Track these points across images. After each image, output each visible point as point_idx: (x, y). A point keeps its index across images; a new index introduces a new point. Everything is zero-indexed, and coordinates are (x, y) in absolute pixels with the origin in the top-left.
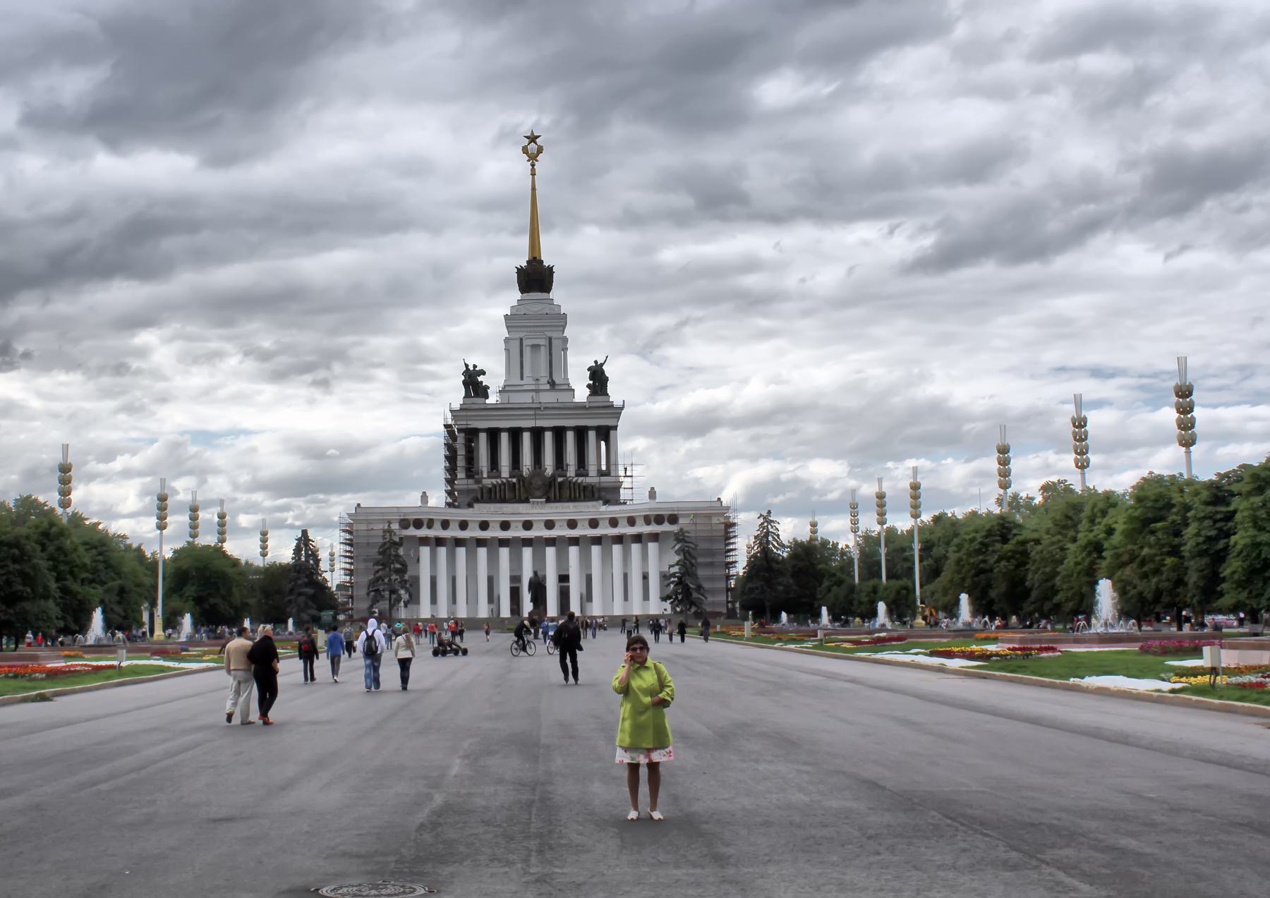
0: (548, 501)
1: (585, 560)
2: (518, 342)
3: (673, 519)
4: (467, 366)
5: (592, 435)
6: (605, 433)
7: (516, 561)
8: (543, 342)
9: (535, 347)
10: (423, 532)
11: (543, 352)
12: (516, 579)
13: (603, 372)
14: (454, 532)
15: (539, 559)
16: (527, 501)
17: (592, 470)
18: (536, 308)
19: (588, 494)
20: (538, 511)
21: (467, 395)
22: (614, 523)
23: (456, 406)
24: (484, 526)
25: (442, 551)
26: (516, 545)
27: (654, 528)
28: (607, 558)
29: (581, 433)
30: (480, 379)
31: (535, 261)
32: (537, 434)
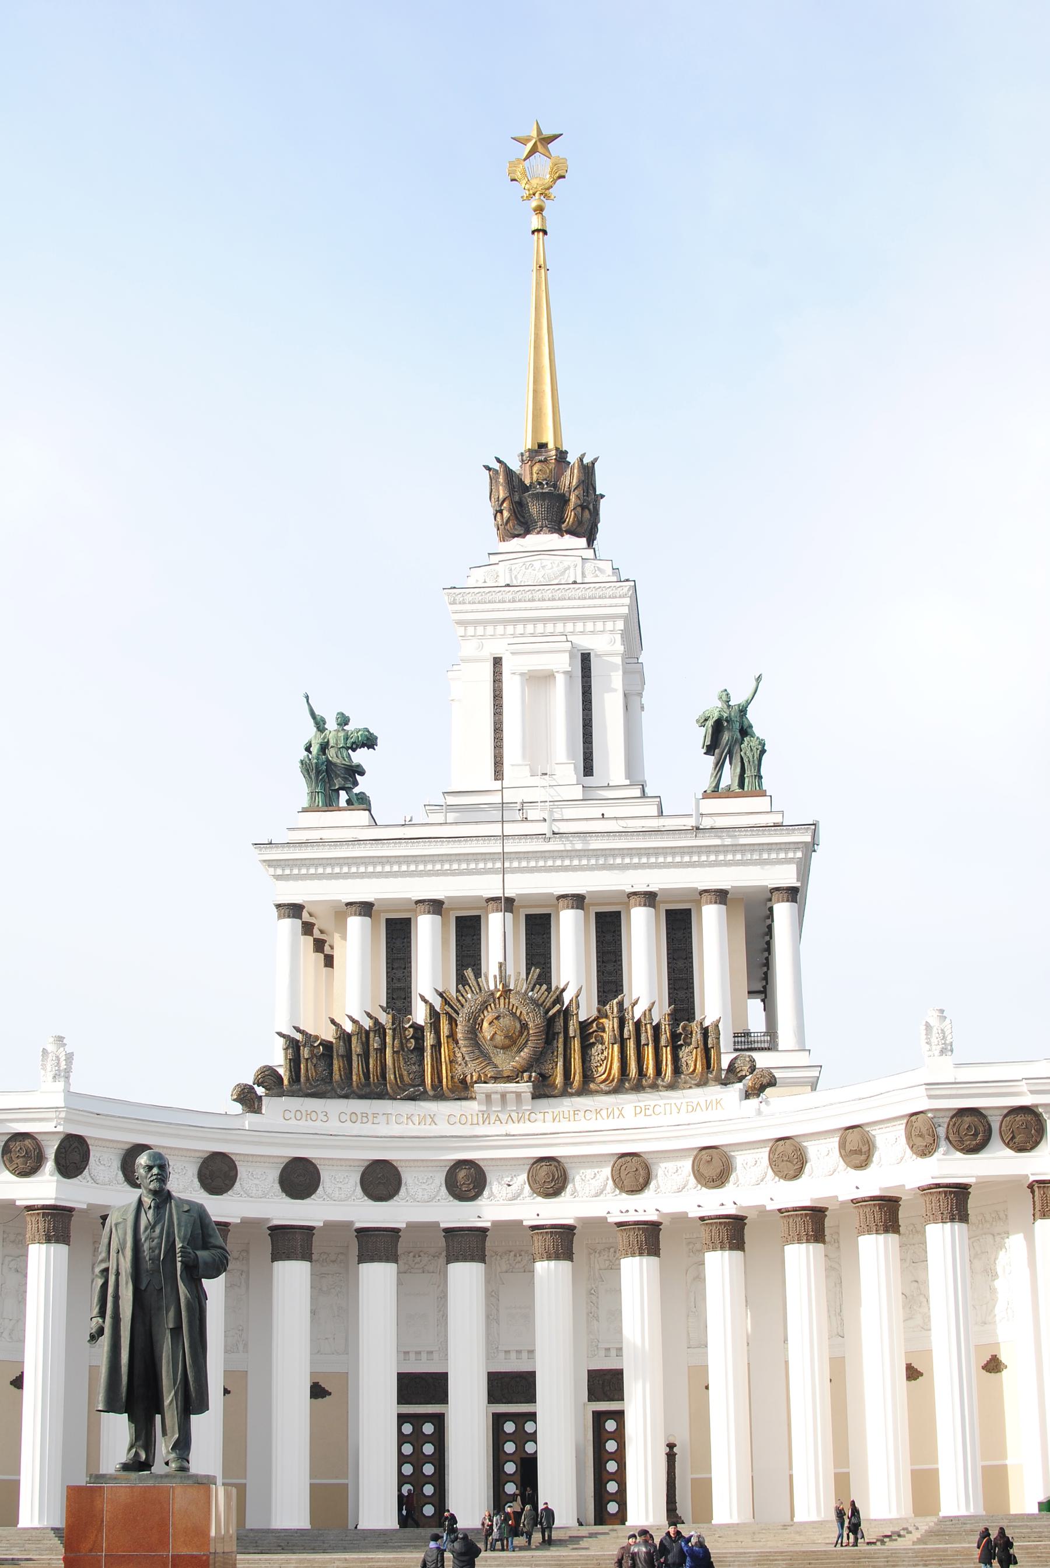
0: (543, 1090)
1: (683, 1304)
2: (489, 667)
3: (1026, 1128)
4: (320, 724)
7: (421, 1311)
8: (562, 663)
10: (45, 1188)
12: (423, 1388)
13: (745, 731)
16: (462, 1090)
19: (690, 1056)
20: (502, 1125)
22: (789, 1158)
24: (300, 1178)
27: (952, 1166)
28: (763, 1297)
30: (359, 757)
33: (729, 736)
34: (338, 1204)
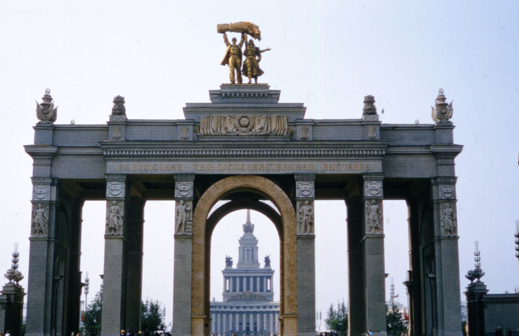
5: (265, 279)
6: (270, 277)
8: (250, 248)
9: (248, 250)
11: (250, 252)
14: (223, 309)
15: (248, 317)
17: (265, 290)
18: (248, 237)
21: (227, 265)
22: (271, 307)
23: (223, 269)
24: (231, 307)
25: (219, 315)
26: (241, 313)
29: (262, 278)
31: (249, 222)
32: (248, 278)
33: (267, 261)
34: (235, 310)
